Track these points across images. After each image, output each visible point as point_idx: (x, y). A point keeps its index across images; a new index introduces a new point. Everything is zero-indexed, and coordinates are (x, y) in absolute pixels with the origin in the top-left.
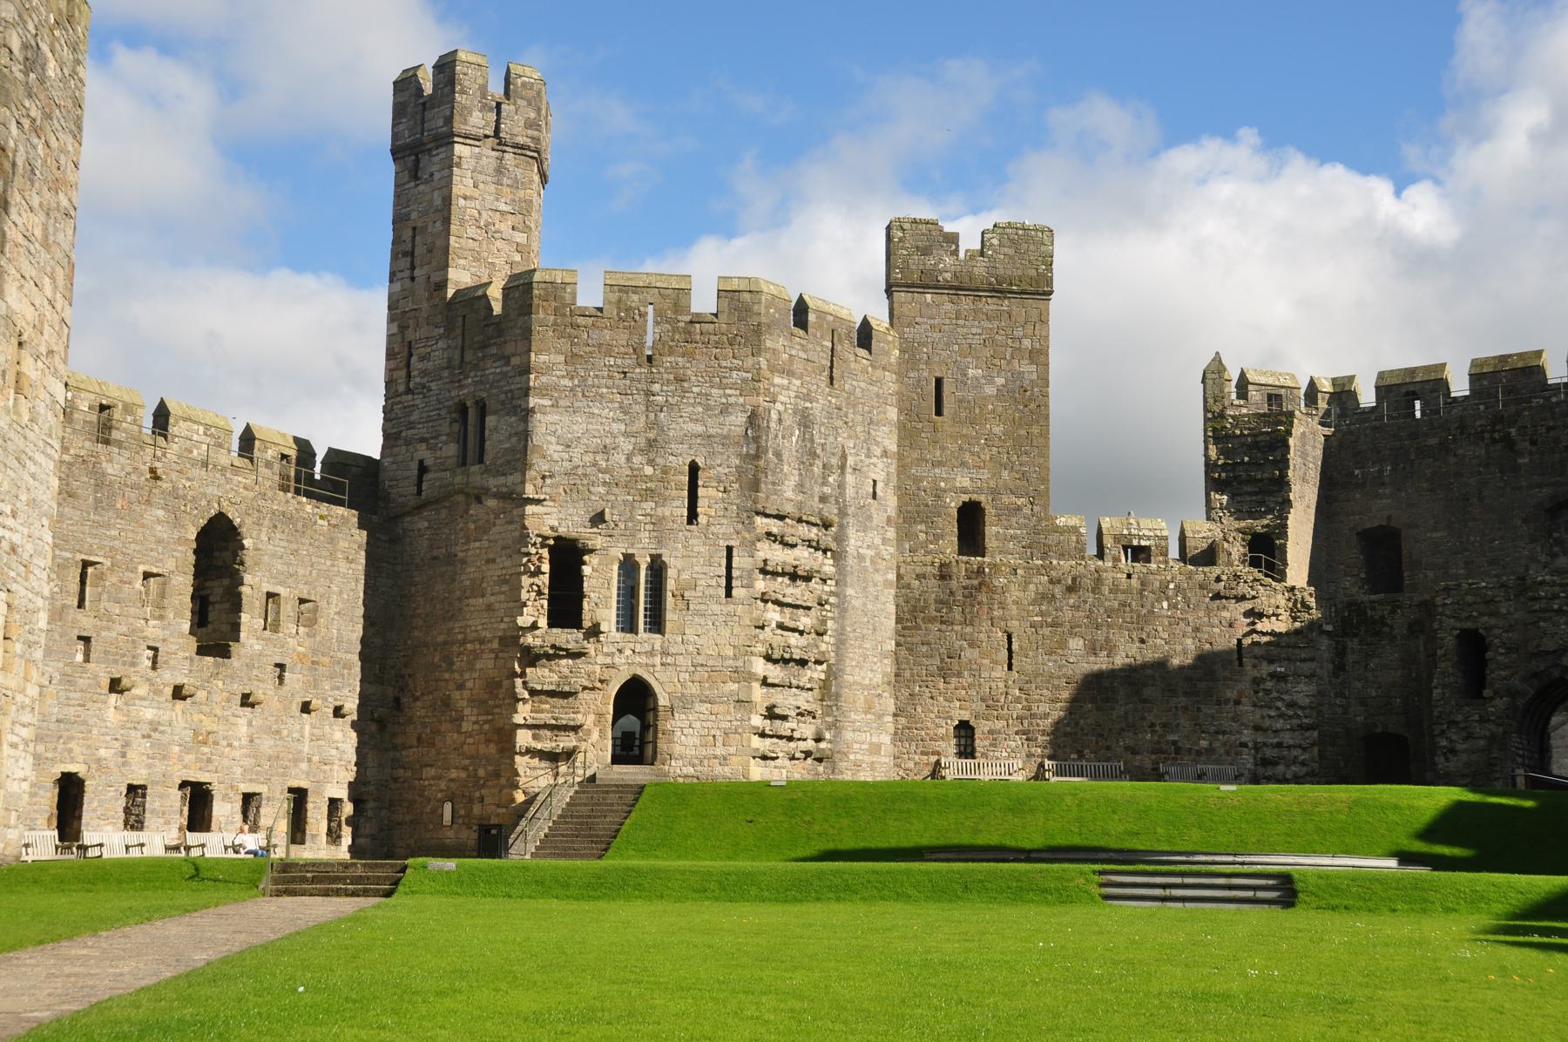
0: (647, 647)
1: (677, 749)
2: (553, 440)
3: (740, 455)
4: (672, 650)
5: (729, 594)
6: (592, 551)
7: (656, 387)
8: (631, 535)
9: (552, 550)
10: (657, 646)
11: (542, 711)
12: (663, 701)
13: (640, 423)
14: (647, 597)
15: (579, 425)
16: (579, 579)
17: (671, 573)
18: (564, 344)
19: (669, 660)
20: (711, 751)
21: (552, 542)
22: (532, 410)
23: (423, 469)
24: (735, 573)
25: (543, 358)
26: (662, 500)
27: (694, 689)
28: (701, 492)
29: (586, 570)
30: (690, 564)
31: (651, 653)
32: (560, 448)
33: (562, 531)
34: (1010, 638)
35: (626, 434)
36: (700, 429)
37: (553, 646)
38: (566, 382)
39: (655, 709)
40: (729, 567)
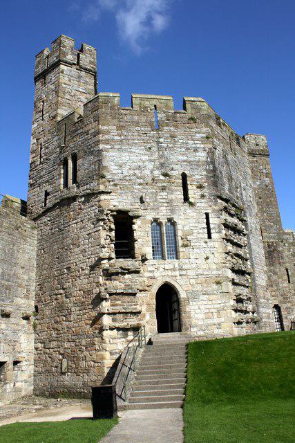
0: (171, 266)
1: (194, 322)
2: (113, 164)
3: (206, 170)
4: (185, 267)
5: (210, 237)
6: (138, 217)
7: (162, 140)
8: (156, 209)
9: (113, 216)
10: (177, 266)
11: (116, 305)
12: (182, 295)
13: (155, 156)
14: (168, 241)
15: (125, 157)
16: (132, 231)
17: (179, 227)
18: (115, 121)
19: (184, 273)
20: (210, 321)
21: (115, 213)
22: (102, 150)
23: (47, 194)
24: (211, 226)
25: (105, 128)
26: (172, 192)
27: (199, 288)
28: (189, 187)
29: (135, 227)
30: (189, 221)
31: (174, 269)
32: (116, 167)
33: (120, 207)
34: (287, 270)
35: (150, 161)
36: (185, 158)
37: (121, 268)
38: (117, 138)
39: (178, 301)
40: (208, 223)
